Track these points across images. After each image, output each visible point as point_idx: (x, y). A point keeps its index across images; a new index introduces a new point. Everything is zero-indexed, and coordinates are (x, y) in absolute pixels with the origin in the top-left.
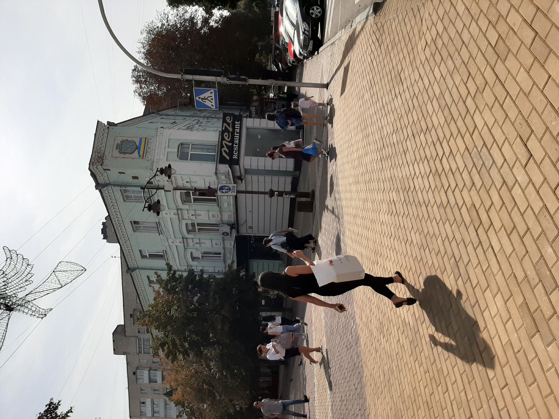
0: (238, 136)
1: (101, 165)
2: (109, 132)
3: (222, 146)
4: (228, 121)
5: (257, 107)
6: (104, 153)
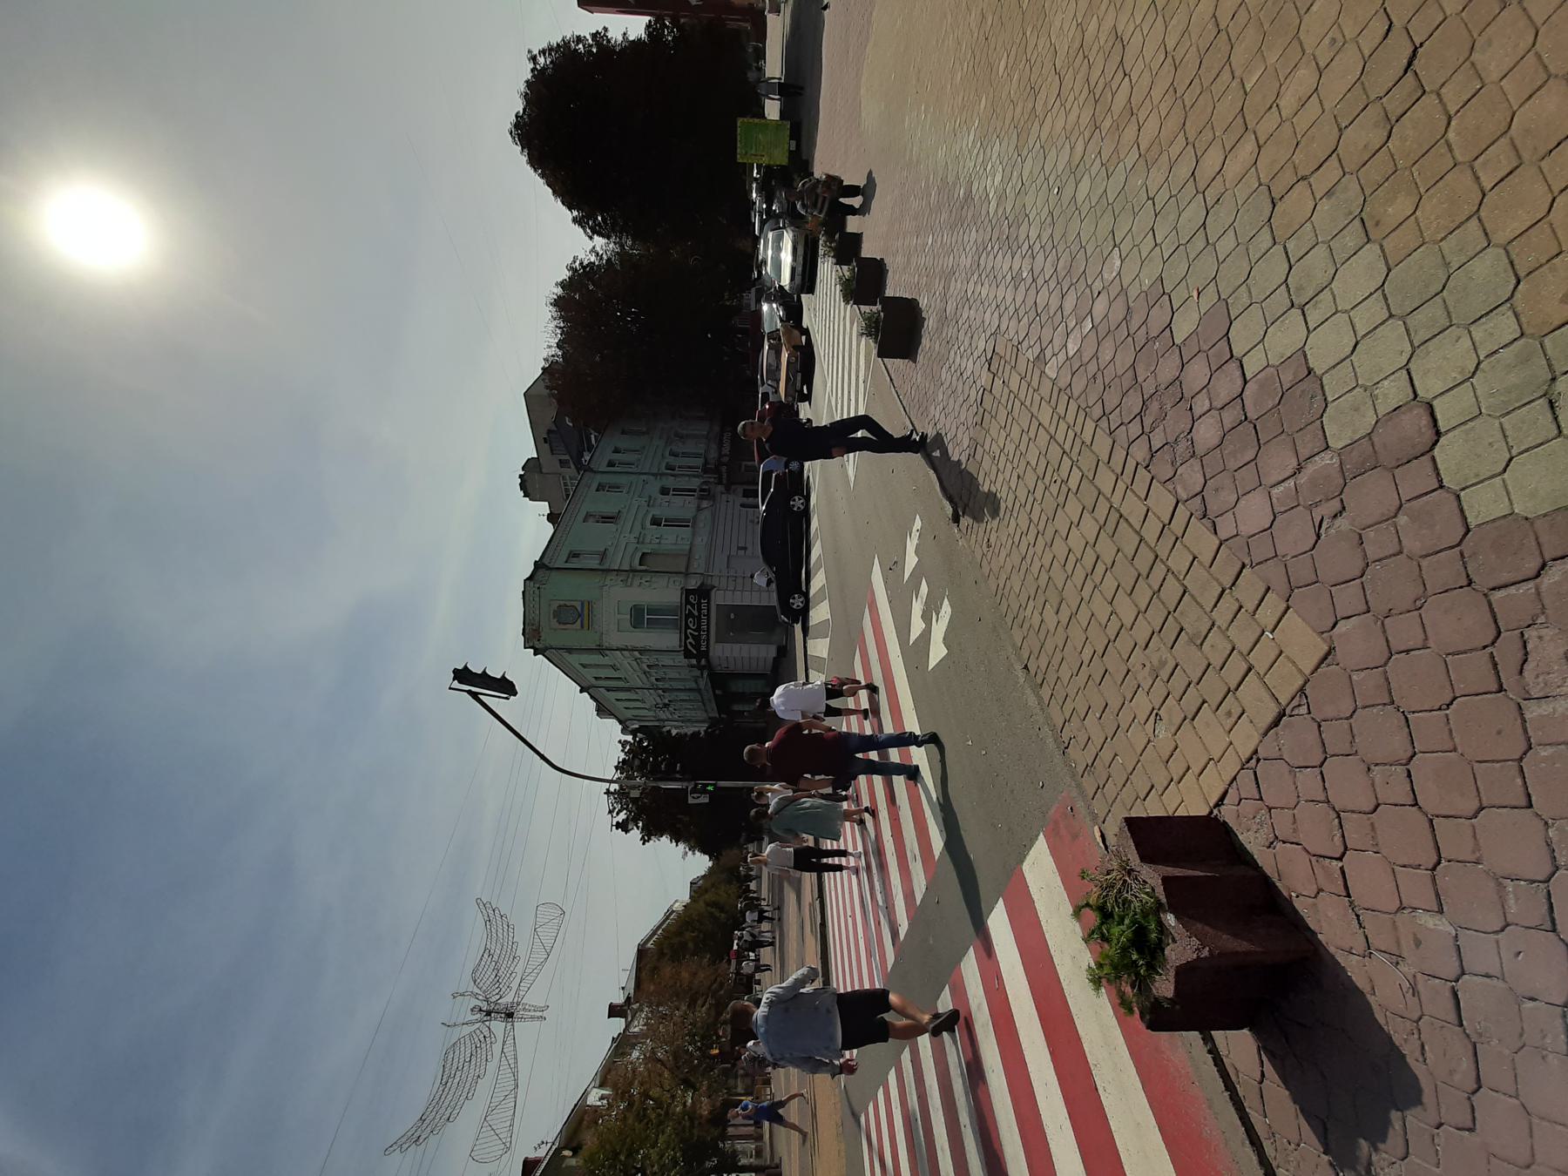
1: (539, 640)
4: (692, 601)
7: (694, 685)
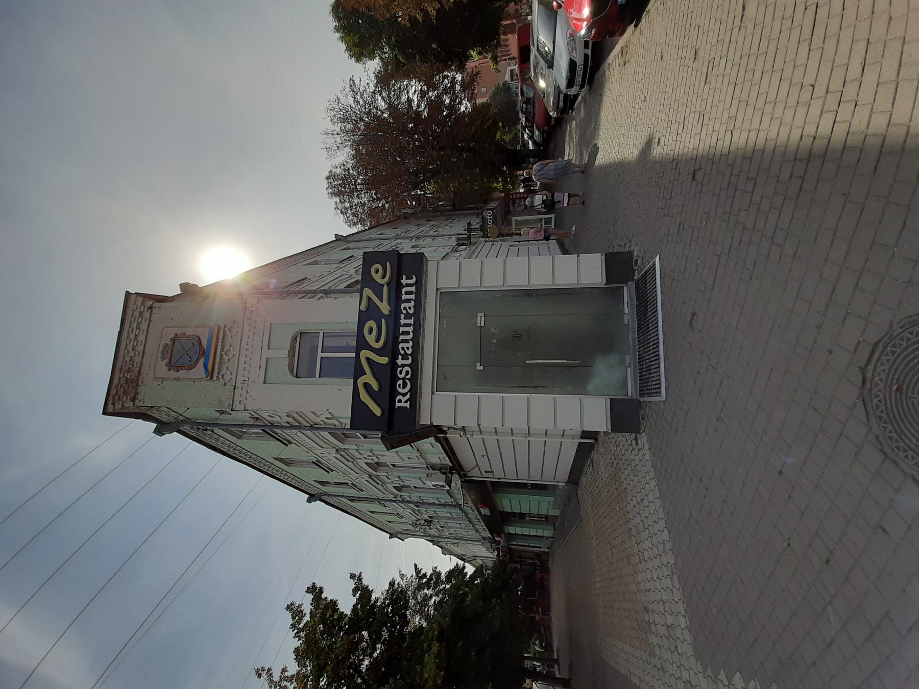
0: (408, 325)
3: (358, 372)
4: (377, 278)
5: (495, 210)
6: (140, 368)
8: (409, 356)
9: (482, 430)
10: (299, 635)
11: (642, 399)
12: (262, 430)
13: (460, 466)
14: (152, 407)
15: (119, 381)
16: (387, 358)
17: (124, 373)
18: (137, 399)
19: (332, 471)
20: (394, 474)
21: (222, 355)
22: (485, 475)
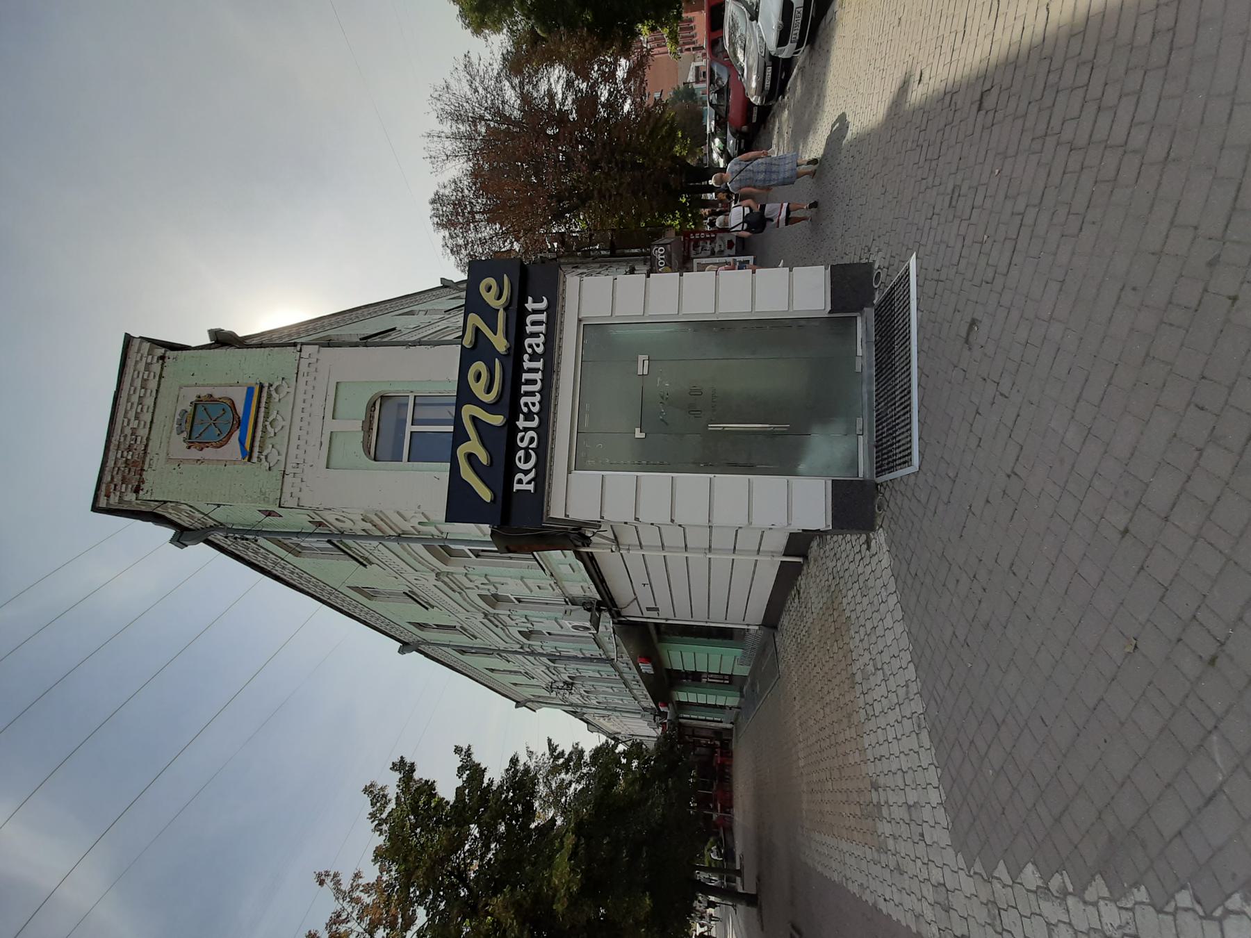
0: (535, 370)
2: (163, 375)
3: (460, 436)
4: (490, 298)
6: (146, 446)
7: (592, 650)
8: (535, 416)
9: (643, 543)
10: (380, 827)
11: (880, 480)
12: (329, 542)
13: (612, 599)
14: (165, 502)
15: (115, 463)
16: (502, 417)
17: (123, 452)
18: (142, 490)
19: (433, 607)
20: (520, 612)
21: (265, 427)
22: (647, 614)
